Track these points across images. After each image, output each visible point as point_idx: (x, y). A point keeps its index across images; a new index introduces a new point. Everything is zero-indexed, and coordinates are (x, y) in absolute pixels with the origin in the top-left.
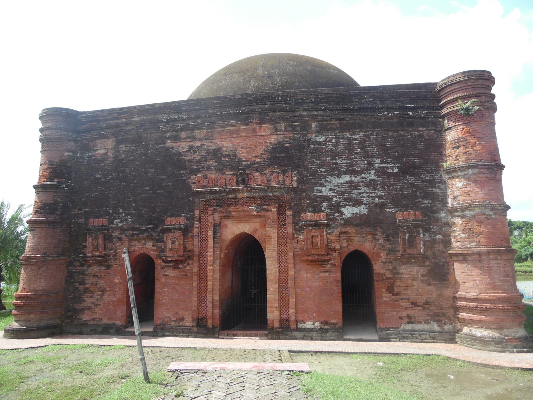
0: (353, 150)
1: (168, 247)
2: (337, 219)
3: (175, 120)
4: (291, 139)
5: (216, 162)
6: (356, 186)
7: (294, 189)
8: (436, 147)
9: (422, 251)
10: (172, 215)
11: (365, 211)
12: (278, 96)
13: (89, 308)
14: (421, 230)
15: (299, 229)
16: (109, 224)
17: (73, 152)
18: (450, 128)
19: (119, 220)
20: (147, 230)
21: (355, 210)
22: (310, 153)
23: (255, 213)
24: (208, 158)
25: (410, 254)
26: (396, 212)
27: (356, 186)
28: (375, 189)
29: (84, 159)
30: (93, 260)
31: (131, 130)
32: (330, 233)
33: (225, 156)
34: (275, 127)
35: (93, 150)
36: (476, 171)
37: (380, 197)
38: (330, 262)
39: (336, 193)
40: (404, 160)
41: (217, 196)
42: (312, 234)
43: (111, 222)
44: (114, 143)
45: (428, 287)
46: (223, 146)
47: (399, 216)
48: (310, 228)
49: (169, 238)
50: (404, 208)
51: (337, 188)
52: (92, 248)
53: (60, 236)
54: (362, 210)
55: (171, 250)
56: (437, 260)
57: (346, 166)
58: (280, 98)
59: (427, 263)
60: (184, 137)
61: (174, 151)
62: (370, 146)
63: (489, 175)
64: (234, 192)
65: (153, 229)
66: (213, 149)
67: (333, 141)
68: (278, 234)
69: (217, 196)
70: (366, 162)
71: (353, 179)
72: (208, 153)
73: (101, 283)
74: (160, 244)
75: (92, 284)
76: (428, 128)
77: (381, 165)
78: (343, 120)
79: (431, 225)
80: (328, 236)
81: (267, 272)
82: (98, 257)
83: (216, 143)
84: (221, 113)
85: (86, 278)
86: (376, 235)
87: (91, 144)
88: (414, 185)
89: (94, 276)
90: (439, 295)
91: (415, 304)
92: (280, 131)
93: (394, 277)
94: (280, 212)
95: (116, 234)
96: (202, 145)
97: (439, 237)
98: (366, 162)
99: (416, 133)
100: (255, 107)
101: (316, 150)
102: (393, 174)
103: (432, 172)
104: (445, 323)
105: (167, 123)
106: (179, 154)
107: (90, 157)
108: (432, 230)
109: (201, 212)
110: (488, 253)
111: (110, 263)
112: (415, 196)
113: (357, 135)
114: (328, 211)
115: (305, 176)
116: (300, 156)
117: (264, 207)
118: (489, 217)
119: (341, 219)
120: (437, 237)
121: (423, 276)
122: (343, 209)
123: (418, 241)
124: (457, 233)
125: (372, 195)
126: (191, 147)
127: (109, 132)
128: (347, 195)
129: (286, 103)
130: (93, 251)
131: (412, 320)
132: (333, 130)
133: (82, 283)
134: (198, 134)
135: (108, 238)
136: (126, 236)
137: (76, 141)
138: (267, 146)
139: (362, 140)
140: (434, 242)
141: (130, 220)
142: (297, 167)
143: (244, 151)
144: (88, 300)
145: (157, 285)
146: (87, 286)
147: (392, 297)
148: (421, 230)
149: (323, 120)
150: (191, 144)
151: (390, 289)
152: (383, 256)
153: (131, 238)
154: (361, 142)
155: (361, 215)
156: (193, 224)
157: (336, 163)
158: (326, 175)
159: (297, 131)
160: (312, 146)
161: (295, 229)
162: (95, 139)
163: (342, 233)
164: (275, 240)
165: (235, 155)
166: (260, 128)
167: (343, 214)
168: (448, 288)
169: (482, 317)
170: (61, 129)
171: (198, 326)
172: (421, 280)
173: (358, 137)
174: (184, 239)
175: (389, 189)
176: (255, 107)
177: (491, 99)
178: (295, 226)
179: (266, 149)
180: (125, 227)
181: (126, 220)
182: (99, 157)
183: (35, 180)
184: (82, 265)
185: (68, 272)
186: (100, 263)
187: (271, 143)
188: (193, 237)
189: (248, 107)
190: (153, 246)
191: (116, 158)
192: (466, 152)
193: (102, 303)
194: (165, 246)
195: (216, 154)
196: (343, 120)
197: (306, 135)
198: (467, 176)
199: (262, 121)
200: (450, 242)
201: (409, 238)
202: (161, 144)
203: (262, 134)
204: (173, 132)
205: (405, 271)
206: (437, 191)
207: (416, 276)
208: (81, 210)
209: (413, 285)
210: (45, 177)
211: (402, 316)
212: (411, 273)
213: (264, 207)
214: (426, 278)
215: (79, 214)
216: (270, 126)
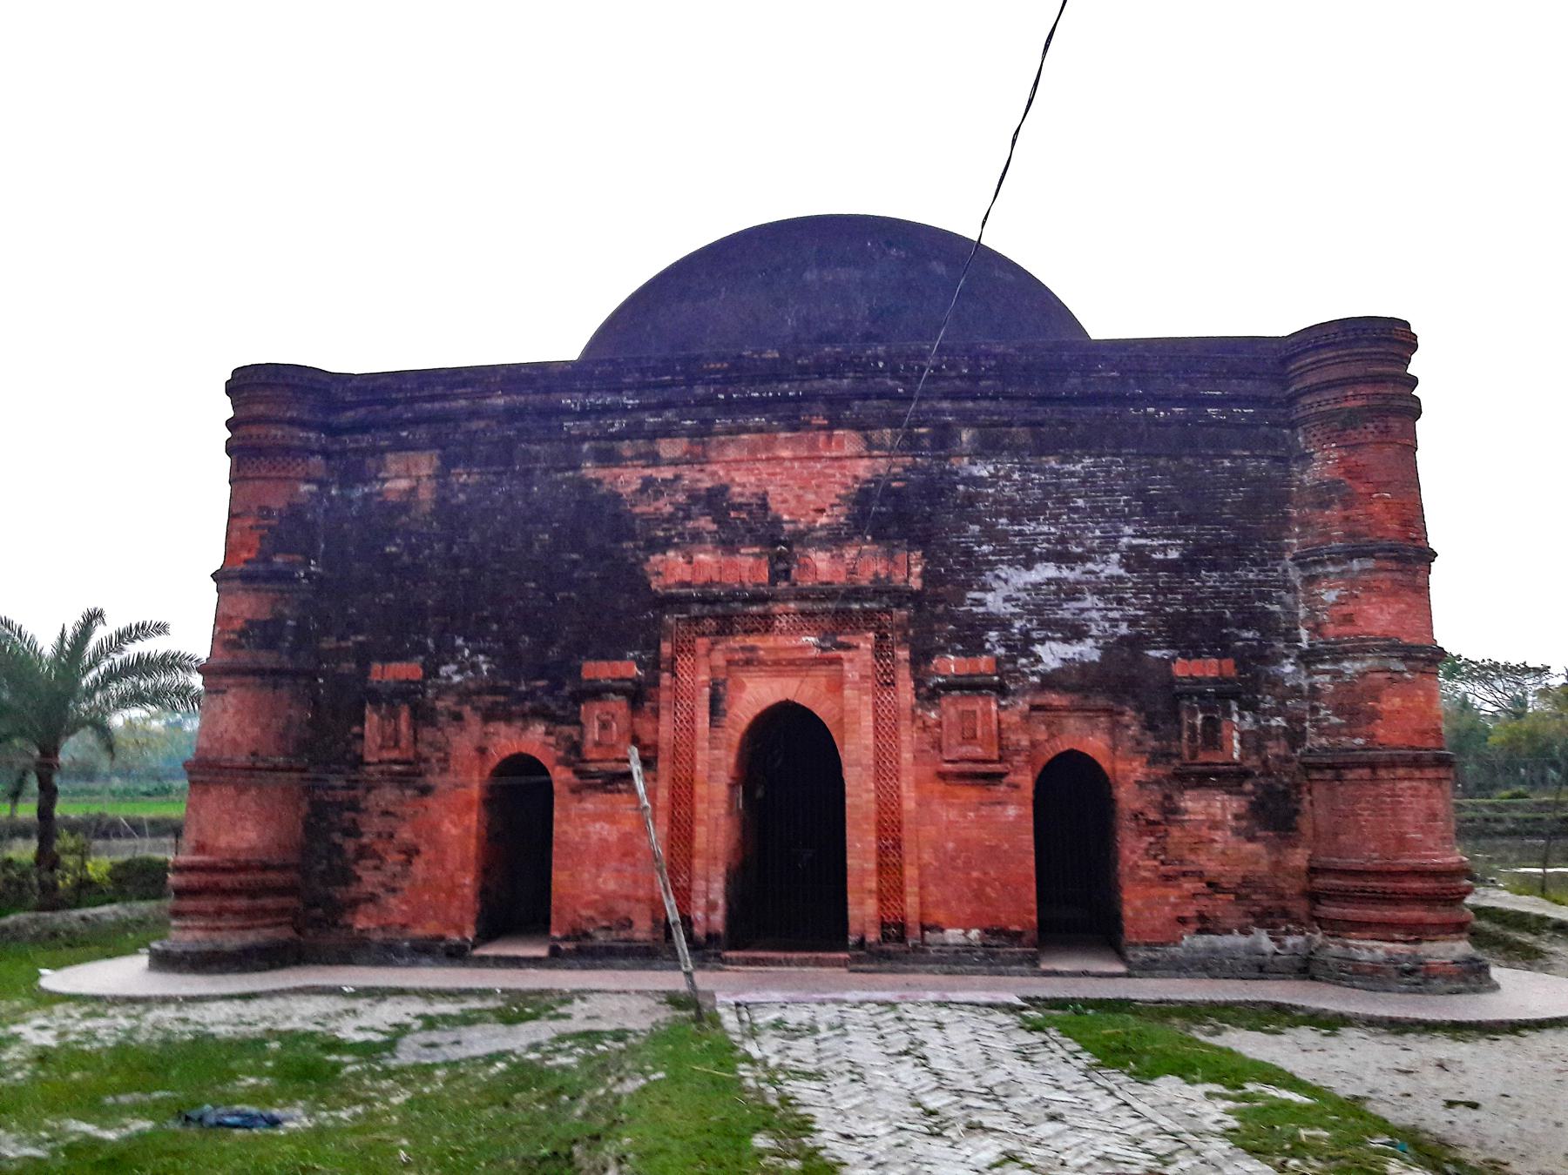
0: (1064, 500)
1: (589, 737)
2: (1024, 674)
3: (606, 410)
4: (906, 469)
5: (714, 521)
6: (1073, 592)
7: (915, 596)
9: (1236, 756)
10: (602, 656)
11: (1095, 656)
12: (877, 358)
13: (372, 898)
14: (1234, 706)
15: (929, 695)
16: (426, 677)
17: (322, 484)
19: (453, 667)
20: (531, 694)
22: (956, 506)
23: (815, 653)
24: (695, 510)
25: (1207, 764)
26: (1173, 659)
27: (1073, 592)
28: (1120, 601)
29: (351, 502)
30: (382, 773)
31: (483, 431)
32: (1005, 708)
33: (739, 507)
34: (866, 438)
35: (377, 479)
36: (1370, 564)
37: (1133, 622)
38: (1005, 780)
39: (1022, 607)
40: (1192, 530)
41: (719, 609)
42: (960, 707)
43: (431, 671)
44: (436, 462)
45: (1250, 846)
46: (733, 480)
48: (955, 693)
49: (592, 713)
50: (1192, 651)
51: (1023, 595)
52: (379, 740)
53: (290, 706)
54: (1086, 650)
55: (598, 744)
56: (1272, 780)
57: (1048, 541)
58: (881, 364)
59: (1248, 787)
60: (628, 453)
61: (603, 490)
62: (1110, 492)
63: (1399, 576)
65: (549, 691)
66: (708, 489)
67: (1016, 476)
68: (875, 705)
69: (719, 609)
70: (1098, 533)
71: (1066, 573)
72: (693, 497)
73: (405, 834)
74: (567, 730)
75: (379, 835)
76: (1257, 452)
77: (1135, 542)
78: (1041, 424)
79: (1258, 692)
80: (1003, 715)
81: (848, 801)
82: (396, 762)
83: (713, 474)
84: (729, 397)
85: (364, 818)
86: (1122, 714)
87: (371, 463)
88: (1218, 594)
89: (386, 813)
90: (1277, 864)
92: (880, 447)
93: (1166, 819)
96: (677, 478)
97: (1278, 721)
98: (1098, 533)
99: (1227, 463)
100: (816, 384)
101: (971, 500)
102: (1166, 565)
103: (1264, 562)
104: (1288, 932)
105: (584, 414)
106: (617, 497)
107: (366, 498)
108: (1262, 705)
109: (678, 650)
111: (431, 779)
112: (1219, 620)
113: (1075, 463)
114: (1001, 651)
115: (942, 564)
116: (931, 514)
117: (839, 639)
118: (1396, 676)
119: (1033, 673)
120: (1273, 723)
121: (1237, 817)
122: (1038, 649)
123: (1225, 732)
124: (1323, 713)
125: (1111, 615)
126: (648, 483)
127: (422, 433)
129: (895, 374)
130: (382, 747)
131: (1209, 925)
132: (1016, 450)
133: (353, 831)
134: (669, 448)
135: (423, 716)
136: (475, 709)
137: (327, 455)
138: (846, 486)
139: (1087, 479)
140: (1265, 734)
141: (484, 667)
142: (923, 541)
144: (370, 879)
146: (365, 840)
147: (1162, 868)
148: (1234, 706)
149: (993, 425)
150: (648, 472)
153: (489, 716)
154: (1083, 482)
155: (1083, 664)
156: (657, 678)
157: (1020, 533)
158: (997, 562)
159: (923, 449)
160: (961, 487)
161: (917, 695)
162: (383, 451)
163: (1034, 708)
164: (868, 721)
165: (764, 506)
166: (830, 438)
167: (1039, 660)
168: (1296, 846)
172: (1232, 828)
173: (1078, 467)
174: (633, 716)
175: (1156, 602)
176: (816, 384)
177: (1406, 391)
178: (917, 688)
179: (843, 492)
180: (472, 685)
181: (475, 667)
182: (392, 498)
185: (312, 803)
186: (401, 780)
187: (856, 478)
188: (656, 713)
189: (796, 384)
190: (548, 733)
191: (442, 502)
192: (1347, 518)
193: (406, 884)
194: (582, 735)
195: (715, 500)
196: (1041, 424)
197: (947, 459)
198: (1348, 576)
199: (834, 423)
201: (1203, 725)
202: (567, 469)
203: (834, 454)
204: (597, 439)
205: (1193, 804)
206: (1276, 608)
207: (1219, 818)
208: (342, 638)
209: (1213, 841)
211: (1186, 914)
212: (1212, 810)
213: (839, 639)
214: (1244, 823)
215: (339, 649)
216: (853, 434)
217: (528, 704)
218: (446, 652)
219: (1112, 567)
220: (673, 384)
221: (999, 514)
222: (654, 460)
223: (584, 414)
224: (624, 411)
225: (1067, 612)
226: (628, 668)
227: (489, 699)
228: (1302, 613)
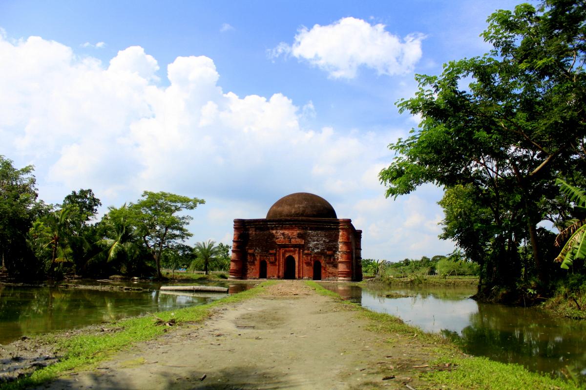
8: (337, 236)
21: (317, 250)
27: (318, 244)
50: (329, 251)
54: (319, 250)
91: (330, 273)
94: (299, 250)
95: (256, 254)
105: (270, 224)
127: (253, 226)
128: (316, 247)
134: (278, 228)
139: (320, 233)
145: (268, 268)
151: (324, 270)
152: (323, 262)
183: (233, 239)
219: (322, 242)
222: (277, 230)
225: (317, 246)
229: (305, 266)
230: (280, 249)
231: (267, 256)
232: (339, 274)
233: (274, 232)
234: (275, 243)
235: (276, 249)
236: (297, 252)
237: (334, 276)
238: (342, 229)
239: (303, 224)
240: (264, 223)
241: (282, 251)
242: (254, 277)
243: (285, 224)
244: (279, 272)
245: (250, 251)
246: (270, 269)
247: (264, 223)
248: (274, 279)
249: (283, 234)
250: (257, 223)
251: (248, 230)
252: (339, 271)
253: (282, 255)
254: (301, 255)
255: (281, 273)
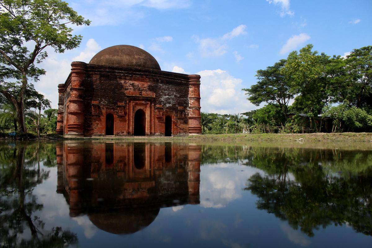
0: (169, 89)
11: (171, 106)
16: (99, 103)
18: (191, 87)
21: (169, 105)
27: (169, 99)
28: (174, 100)
29: (88, 80)
33: (136, 86)
41: (134, 98)
43: (100, 103)
47: (179, 108)
50: (180, 106)
54: (171, 105)
55: (120, 112)
64: (138, 97)
65: (114, 106)
69: (134, 98)
91: (181, 129)
94: (151, 104)
102: (178, 97)
105: (118, 73)
107: (90, 80)
110: (197, 117)
127: (98, 73)
133: (91, 121)
134: (127, 78)
135: (99, 108)
137: (86, 74)
142: (155, 92)
143: (141, 85)
146: (92, 122)
151: (176, 125)
167: (166, 106)
169: (195, 131)
170: (83, 70)
171: (128, 134)
180: (105, 104)
181: (105, 102)
184: (90, 116)
192: (194, 94)
193: (97, 128)
200: (189, 115)
210: (78, 85)
217: (112, 107)
218: (102, 100)
220: (128, 70)
221: (163, 90)
222: (126, 79)
223: (118, 73)
224: (123, 73)
226: (123, 104)
227: (107, 106)
228: (189, 103)
229: (157, 121)
230: (130, 102)
231: (113, 109)
232: (189, 130)
233: (123, 82)
234: (124, 94)
235: (126, 101)
236: (148, 106)
237: (185, 132)
238: (193, 85)
239: (155, 76)
240: (110, 70)
241: (132, 104)
242: (99, 133)
243: (135, 74)
244: (129, 128)
245: (94, 102)
246: (117, 124)
247: (110, 70)
248: (124, 135)
249: (133, 85)
250: (102, 70)
251: (89, 76)
252: (190, 126)
253: (132, 108)
254: (153, 109)
255: (131, 128)
